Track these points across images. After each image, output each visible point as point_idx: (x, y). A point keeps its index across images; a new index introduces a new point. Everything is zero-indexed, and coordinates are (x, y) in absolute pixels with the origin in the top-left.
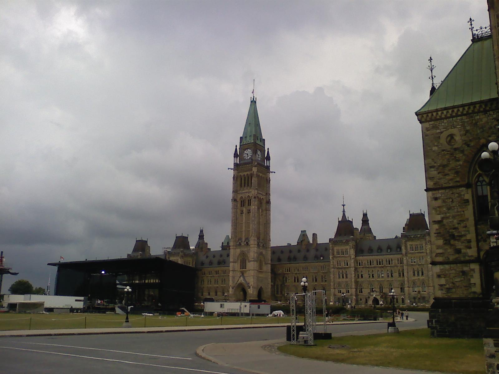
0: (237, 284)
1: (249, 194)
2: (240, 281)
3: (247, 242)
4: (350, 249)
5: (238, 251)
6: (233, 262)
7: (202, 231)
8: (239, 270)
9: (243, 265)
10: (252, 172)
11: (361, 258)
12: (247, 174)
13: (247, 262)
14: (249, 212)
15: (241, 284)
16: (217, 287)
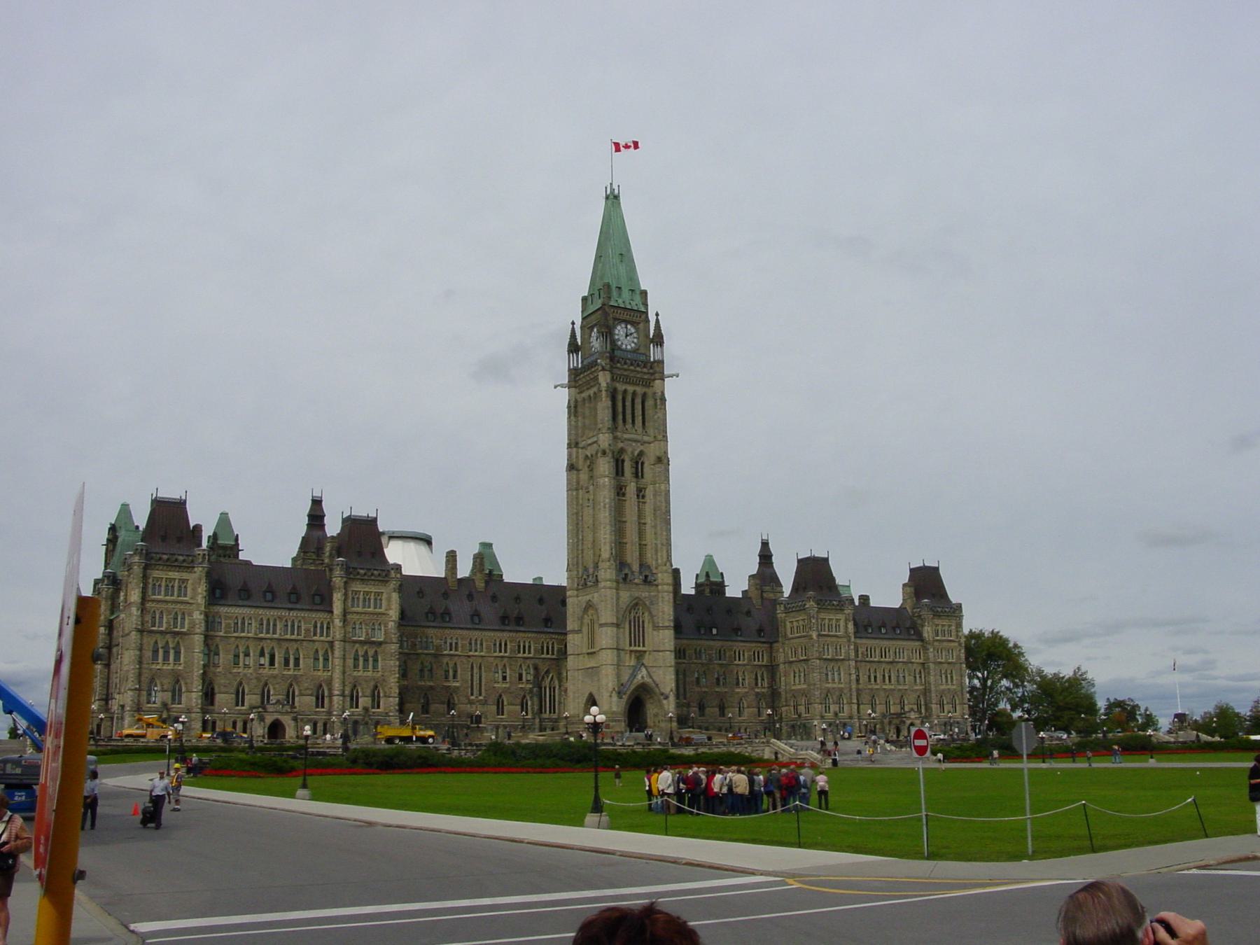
0: (633, 687)
1: (642, 448)
2: (639, 677)
3: (646, 577)
4: (846, 620)
5: (625, 596)
6: (618, 626)
7: (317, 503)
8: (627, 648)
9: (637, 635)
10: (649, 391)
11: (858, 641)
12: (634, 393)
13: (648, 627)
14: (640, 493)
15: (643, 688)
16: (431, 688)
